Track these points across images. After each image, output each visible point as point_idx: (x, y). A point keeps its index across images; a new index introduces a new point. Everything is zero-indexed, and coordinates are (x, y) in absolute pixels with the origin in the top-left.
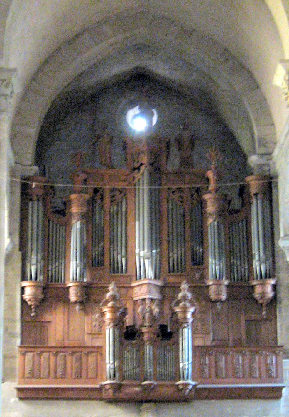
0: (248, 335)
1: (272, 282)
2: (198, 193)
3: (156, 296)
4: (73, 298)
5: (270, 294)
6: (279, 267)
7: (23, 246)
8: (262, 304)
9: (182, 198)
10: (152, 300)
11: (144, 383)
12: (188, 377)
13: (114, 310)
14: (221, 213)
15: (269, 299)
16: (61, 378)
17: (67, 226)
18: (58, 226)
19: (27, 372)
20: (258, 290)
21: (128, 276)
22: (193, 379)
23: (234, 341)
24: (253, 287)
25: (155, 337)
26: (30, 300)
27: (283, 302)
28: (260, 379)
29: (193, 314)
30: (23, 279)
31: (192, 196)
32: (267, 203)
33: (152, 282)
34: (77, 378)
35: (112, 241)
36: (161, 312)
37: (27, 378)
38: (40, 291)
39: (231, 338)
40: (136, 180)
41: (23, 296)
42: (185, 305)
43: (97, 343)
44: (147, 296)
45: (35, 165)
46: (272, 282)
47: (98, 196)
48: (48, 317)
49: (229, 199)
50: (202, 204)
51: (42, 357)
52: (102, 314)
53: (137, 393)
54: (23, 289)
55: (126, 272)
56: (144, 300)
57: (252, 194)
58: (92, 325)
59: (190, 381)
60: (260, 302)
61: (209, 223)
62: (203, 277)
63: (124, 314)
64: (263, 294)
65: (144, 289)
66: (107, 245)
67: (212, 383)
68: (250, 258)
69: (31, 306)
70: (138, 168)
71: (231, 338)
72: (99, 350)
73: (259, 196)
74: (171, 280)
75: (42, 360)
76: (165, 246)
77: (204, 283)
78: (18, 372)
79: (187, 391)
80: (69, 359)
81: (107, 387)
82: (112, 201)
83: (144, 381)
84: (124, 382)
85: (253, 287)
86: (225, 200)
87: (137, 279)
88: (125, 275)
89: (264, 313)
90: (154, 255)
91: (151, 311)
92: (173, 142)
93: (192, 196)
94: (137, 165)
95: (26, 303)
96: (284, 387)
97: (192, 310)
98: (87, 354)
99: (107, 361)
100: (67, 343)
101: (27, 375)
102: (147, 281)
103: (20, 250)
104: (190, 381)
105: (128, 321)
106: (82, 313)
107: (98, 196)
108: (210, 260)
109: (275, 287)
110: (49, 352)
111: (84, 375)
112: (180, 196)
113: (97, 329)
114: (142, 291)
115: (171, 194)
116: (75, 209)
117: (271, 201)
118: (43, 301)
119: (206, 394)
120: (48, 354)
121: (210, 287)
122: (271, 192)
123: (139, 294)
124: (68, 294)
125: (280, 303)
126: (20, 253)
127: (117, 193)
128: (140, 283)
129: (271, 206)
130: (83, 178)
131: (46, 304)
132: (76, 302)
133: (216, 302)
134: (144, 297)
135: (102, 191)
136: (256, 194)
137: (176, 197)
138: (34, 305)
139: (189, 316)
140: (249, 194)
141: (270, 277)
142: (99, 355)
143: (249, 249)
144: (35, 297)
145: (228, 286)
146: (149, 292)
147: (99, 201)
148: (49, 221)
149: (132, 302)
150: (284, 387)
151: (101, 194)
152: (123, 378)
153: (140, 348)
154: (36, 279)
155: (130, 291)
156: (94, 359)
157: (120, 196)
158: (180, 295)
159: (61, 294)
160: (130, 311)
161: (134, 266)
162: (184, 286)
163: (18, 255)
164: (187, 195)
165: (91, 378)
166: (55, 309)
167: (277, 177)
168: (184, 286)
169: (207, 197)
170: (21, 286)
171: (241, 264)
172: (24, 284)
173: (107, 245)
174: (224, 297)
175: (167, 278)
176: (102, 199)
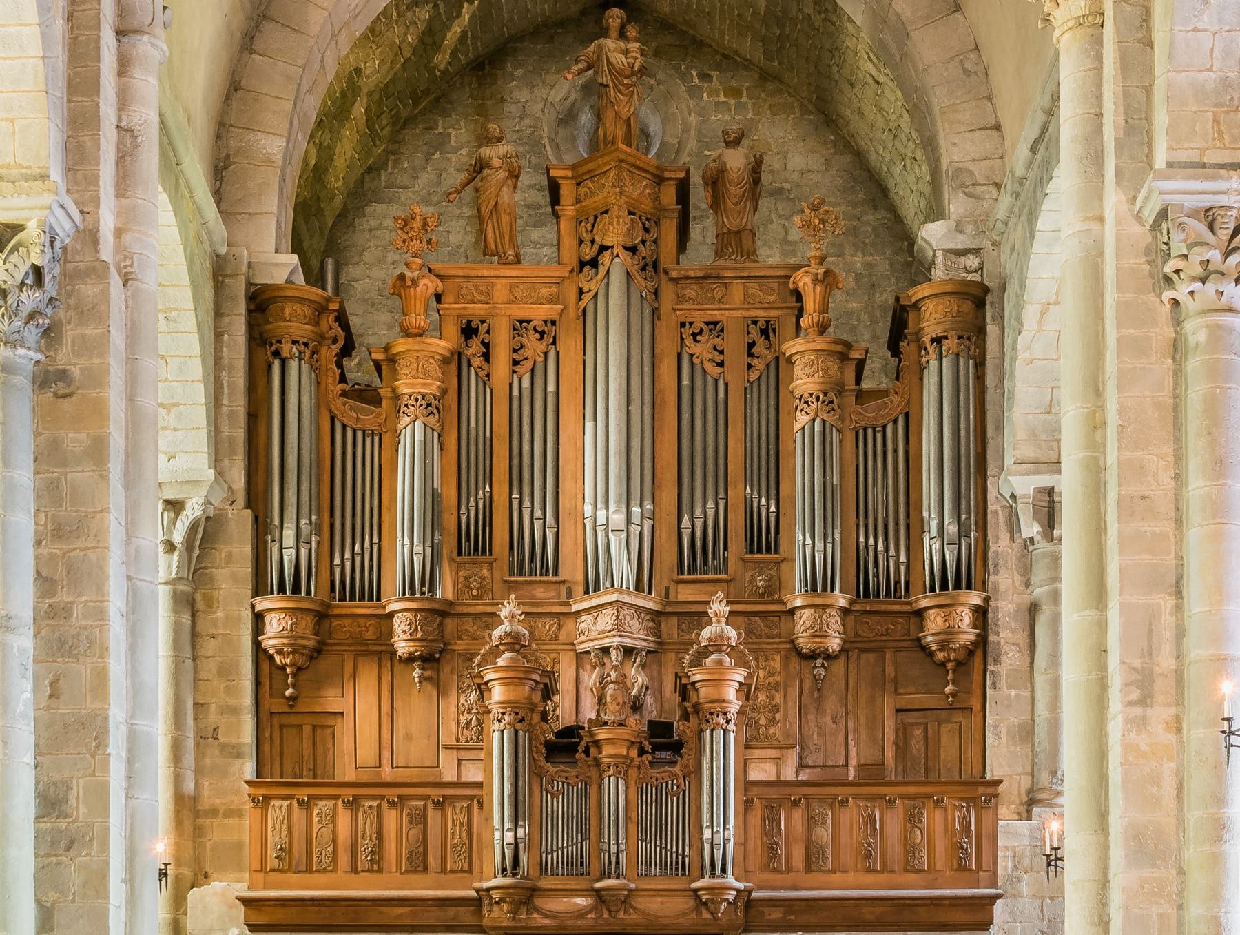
0: (902, 750)
1: (975, 599)
2: (767, 338)
3: (638, 636)
4: (403, 647)
5: (967, 634)
6: (996, 552)
7: (256, 498)
8: (943, 664)
9: (722, 352)
10: (628, 652)
11: (598, 885)
12: (724, 870)
13: (514, 676)
14: (832, 395)
15: (964, 647)
16: (370, 871)
17: (385, 436)
18: (359, 434)
19: (272, 853)
20: (935, 622)
21: (563, 582)
22: (743, 875)
23: (860, 766)
24: (920, 614)
25: (634, 753)
26: (279, 652)
27: (1003, 658)
28: (931, 876)
29: (745, 690)
30: (259, 589)
31: (751, 345)
32: (967, 367)
33: (627, 599)
34: (415, 871)
35: (517, 478)
36: (655, 687)
37: (273, 870)
38: (308, 622)
39: (853, 762)
40: (587, 297)
41: (260, 638)
42: (720, 662)
43: (472, 773)
44: (614, 641)
45: (293, 252)
46: (975, 599)
47: (475, 348)
48: (332, 701)
49: (855, 355)
50: (780, 366)
51: (316, 811)
52: (483, 689)
53: (581, 914)
54: (259, 618)
55: (556, 573)
56: (606, 651)
57: (927, 340)
58: (458, 723)
59: (730, 880)
60: (940, 656)
61: (797, 427)
62: (772, 590)
63: (548, 692)
64: (948, 633)
65: (606, 620)
66: (501, 491)
67: (795, 888)
68: (914, 529)
69: (283, 668)
70: (594, 263)
71: (853, 762)
72: (473, 794)
73: (946, 345)
74: (685, 593)
75: (315, 819)
76: (668, 496)
77: (783, 603)
78: (250, 854)
79: (724, 906)
80: (391, 819)
81: (496, 895)
82: (515, 363)
83: (600, 879)
84: (544, 883)
85: (920, 614)
86: (843, 357)
87: (587, 592)
88: (555, 579)
89: (948, 689)
90: (636, 518)
91: (621, 682)
92: (696, 179)
93: (751, 345)
94: (588, 252)
95: (271, 658)
96: (999, 896)
97: (739, 675)
98: (441, 804)
99: (496, 823)
100: (387, 773)
101: (272, 863)
102: (614, 597)
103: (248, 506)
104: (730, 880)
105: (564, 710)
106: (430, 689)
107: (475, 348)
108: (799, 536)
109: (981, 613)
110: (336, 797)
111: (433, 862)
112: (715, 348)
113: (472, 733)
114: (600, 626)
115: (689, 341)
116: (409, 384)
117: (980, 364)
118: (317, 652)
119: (776, 915)
120: (332, 803)
121: (798, 613)
122: (981, 331)
123: (593, 635)
124: (390, 633)
125: (997, 661)
126: (248, 513)
127: (531, 340)
128: (596, 602)
129: (980, 378)
130: (431, 290)
131: (323, 664)
132: (410, 659)
133: (813, 656)
134: (607, 642)
135: (488, 332)
136: (937, 340)
137: (702, 350)
138: (291, 665)
139: (731, 693)
140: (918, 335)
141: (969, 587)
142: (476, 805)
143: (912, 503)
144: (293, 638)
145: (845, 612)
146: (619, 629)
147: (478, 362)
148: (333, 419)
149: (572, 653)
150: (999, 896)
151: (483, 343)
152: (543, 869)
153: (588, 788)
154: (296, 589)
155: (569, 624)
156: (463, 817)
157: (541, 347)
158: (706, 633)
159: (370, 635)
160: (565, 683)
161: (580, 553)
162: (718, 607)
163: (240, 521)
164: (734, 344)
165: (452, 871)
166: (354, 676)
167: (1003, 287)
168: (718, 607)
169: (792, 347)
170: (253, 607)
171: (887, 550)
172: (263, 604)
173: (501, 491)
174: (834, 644)
175: (672, 587)
176: (486, 357)
